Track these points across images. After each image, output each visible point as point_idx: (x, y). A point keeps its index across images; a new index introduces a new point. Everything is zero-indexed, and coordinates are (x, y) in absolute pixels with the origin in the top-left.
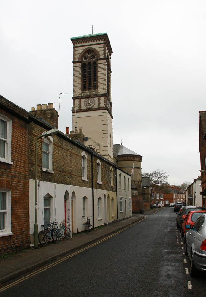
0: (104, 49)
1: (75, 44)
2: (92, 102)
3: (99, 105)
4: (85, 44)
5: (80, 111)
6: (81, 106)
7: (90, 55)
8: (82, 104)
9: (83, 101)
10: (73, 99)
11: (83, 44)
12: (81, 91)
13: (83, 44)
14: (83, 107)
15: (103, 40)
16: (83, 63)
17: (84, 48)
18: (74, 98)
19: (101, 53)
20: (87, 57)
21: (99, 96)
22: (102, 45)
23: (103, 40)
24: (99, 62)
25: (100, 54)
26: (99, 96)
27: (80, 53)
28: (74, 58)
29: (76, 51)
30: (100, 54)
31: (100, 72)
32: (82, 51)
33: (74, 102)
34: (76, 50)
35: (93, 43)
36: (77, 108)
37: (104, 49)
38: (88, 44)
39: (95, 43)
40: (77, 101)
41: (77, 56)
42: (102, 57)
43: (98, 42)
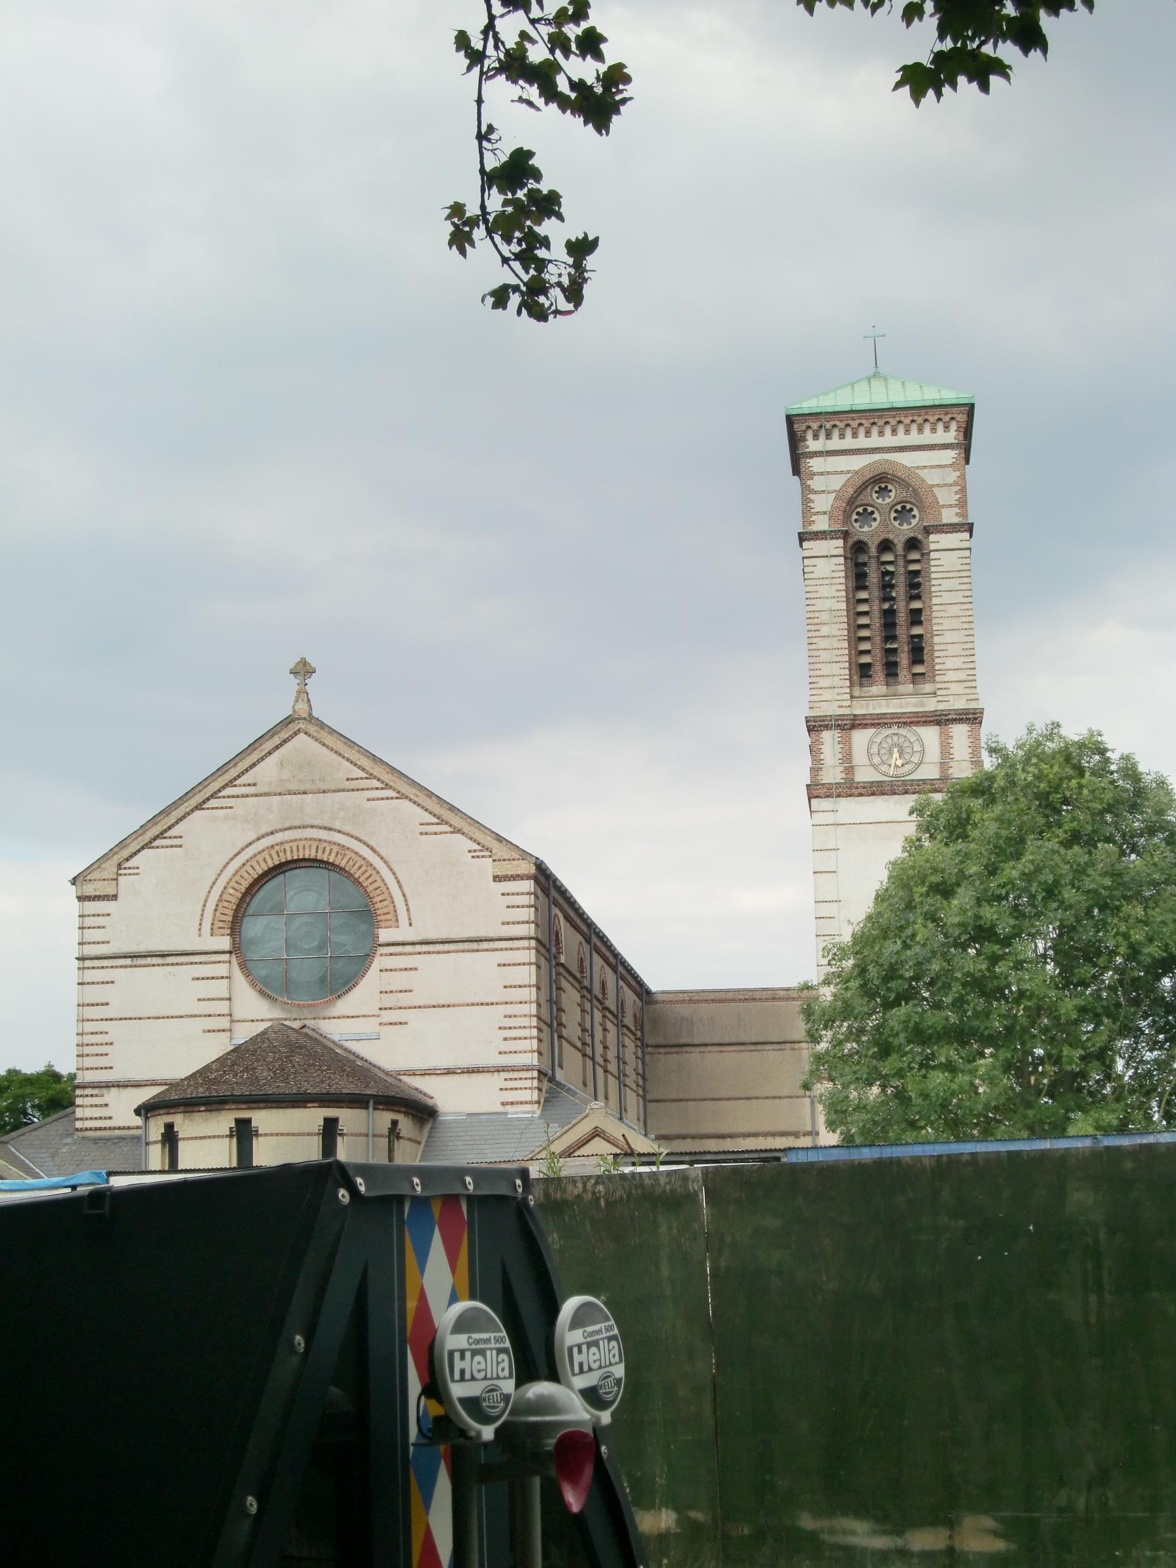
0: (958, 473)
1: (809, 435)
2: (909, 750)
3: (944, 765)
4: (862, 442)
5: (851, 789)
6: (852, 767)
7: (888, 500)
8: (859, 757)
9: (861, 738)
10: (810, 730)
11: (849, 443)
12: (851, 686)
13: (849, 443)
14: (864, 775)
15: (953, 426)
16: (855, 539)
17: (857, 463)
18: (815, 726)
19: (946, 497)
20: (870, 509)
21: (940, 720)
22: (949, 456)
23: (953, 426)
24: (937, 541)
25: (941, 503)
26: (940, 720)
27: (838, 489)
28: (807, 512)
29: (812, 475)
30: (941, 503)
31: (947, 598)
32: (843, 479)
33: (814, 751)
34: (815, 470)
35: (901, 439)
36: (832, 774)
37: (958, 473)
38: (875, 441)
39: (914, 438)
40: (829, 738)
41: (823, 503)
42: (949, 516)
43: (928, 437)
